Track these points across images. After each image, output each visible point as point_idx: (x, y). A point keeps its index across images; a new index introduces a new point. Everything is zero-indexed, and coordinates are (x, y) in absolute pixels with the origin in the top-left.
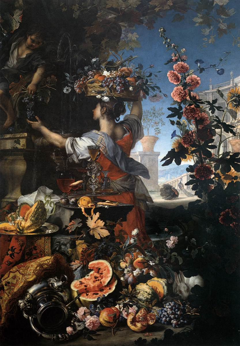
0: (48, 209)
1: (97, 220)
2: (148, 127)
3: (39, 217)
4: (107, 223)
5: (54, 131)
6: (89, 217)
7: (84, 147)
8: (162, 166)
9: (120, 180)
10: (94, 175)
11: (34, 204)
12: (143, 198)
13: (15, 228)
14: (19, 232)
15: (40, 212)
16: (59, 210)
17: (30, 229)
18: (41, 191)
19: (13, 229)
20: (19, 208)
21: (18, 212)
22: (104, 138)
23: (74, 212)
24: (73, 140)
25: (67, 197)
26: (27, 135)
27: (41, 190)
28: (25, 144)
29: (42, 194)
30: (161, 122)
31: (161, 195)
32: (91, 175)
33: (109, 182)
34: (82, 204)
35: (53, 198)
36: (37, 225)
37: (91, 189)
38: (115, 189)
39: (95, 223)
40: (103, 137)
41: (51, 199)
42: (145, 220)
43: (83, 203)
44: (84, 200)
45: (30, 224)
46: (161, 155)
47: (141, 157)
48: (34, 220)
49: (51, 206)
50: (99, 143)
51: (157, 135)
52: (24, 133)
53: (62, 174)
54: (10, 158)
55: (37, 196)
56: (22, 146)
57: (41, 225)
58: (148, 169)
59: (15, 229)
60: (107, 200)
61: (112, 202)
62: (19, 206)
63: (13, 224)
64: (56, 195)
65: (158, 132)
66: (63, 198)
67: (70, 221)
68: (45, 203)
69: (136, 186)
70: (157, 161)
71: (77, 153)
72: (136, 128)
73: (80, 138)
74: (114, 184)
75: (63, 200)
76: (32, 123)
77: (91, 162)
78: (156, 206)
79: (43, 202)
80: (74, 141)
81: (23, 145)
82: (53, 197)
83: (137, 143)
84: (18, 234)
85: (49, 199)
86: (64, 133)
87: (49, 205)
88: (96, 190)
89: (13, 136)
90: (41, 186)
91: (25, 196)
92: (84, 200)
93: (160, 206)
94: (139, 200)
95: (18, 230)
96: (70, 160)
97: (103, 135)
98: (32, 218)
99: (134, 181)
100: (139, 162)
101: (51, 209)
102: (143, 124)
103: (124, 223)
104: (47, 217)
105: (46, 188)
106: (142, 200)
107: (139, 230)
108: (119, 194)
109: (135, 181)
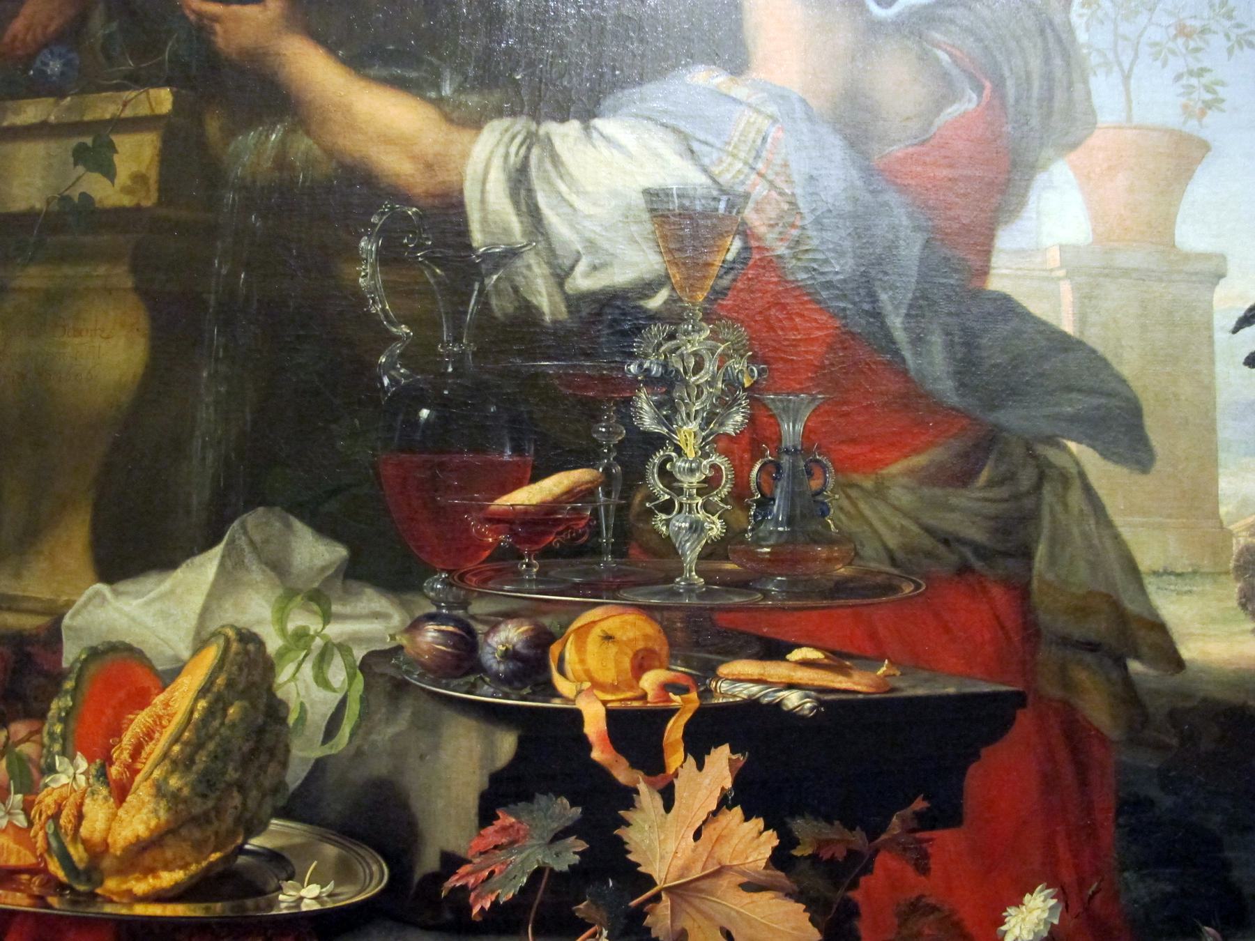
0: (302, 705)
1: (714, 813)
2: (1126, 61)
3: (224, 773)
4: (795, 843)
5: (384, 73)
6: (642, 787)
7: (615, 194)
8: (1247, 369)
9: (911, 472)
10: (693, 426)
11: (186, 654)
12: (1097, 627)
13: (32, 848)
14: (61, 887)
15: (233, 726)
16: (388, 721)
17: (151, 871)
18: (247, 549)
19: (13, 862)
20: (69, 685)
21: (60, 720)
22: (773, 132)
23: (522, 742)
24: (531, 139)
25: (464, 605)
26: (174, 103)
27: (252, 543)
28: (153, 175)
29: (257, 573)
30: (1228, 24)
31: (1243, 606)
32: (669, 421)
33: (819, 493)
34: (588, 672)
35: (348, 610)
36: (205, 841)
37: (667, 548)
38: (870, 550)
39: (697, 835)
40: (774, 120)
41: (327, 617)
42: (1119, 813)
43: (593, 663)
44: (608, 638)
45: (153, 823)
46: (1229, 274)
47: (1076, 288)
48: (186, 792)
49: (323, 682)
50: (739, 165)
51: (1200, 121)
52: (153, 92)
53: (425, 413)
54: (33, 277)
55: (216, 594)
56: (126, 190)
57: (239, 841)
58: (1136, 385)
59: (29, 859)
60: (799, 646)
61: (838, 660)
62: (70, 670)
63: (21, 821)
64: (369, 592)
65: (1208, 97)
66: (431, 618)
67: (486, 816)
68: (282, 653)
69: (1046, 532)
70: (1209, 326)
71: (556, 245)
72: (1035, 64)
73: (587, 128)
74: (862, 505)
75: (430, 633)
76: (215, 19)
77: (673, 317)
78: (1205, 700)
79: (261, 644)
80: (535, 151)
81: (139, 178)
82: (343, 600)
83: (1041, 179)
84: (53, 900)
85: (313, 624)
86: (460, 89)
87: (308, 670)
88: (713, 551)
89: (69, 109)
90: (250, 506)
91: (123, 586)
92: (608, 638)
93: (1235, 698)
94: (1065, 641)
95: (55, 868)
96: (494, 302)
97: (772, 109)
98: (166, 779)
99: (1026, 478)
100: (1068, 326)
101: (320, 703)
102: (1082, 37)
103: (945, 841)
104: (295, 776)
105: (288, 526)
106: (1092, 647)
107: (1063, 895)
108: (908, 589)
109: (1038, 487)
